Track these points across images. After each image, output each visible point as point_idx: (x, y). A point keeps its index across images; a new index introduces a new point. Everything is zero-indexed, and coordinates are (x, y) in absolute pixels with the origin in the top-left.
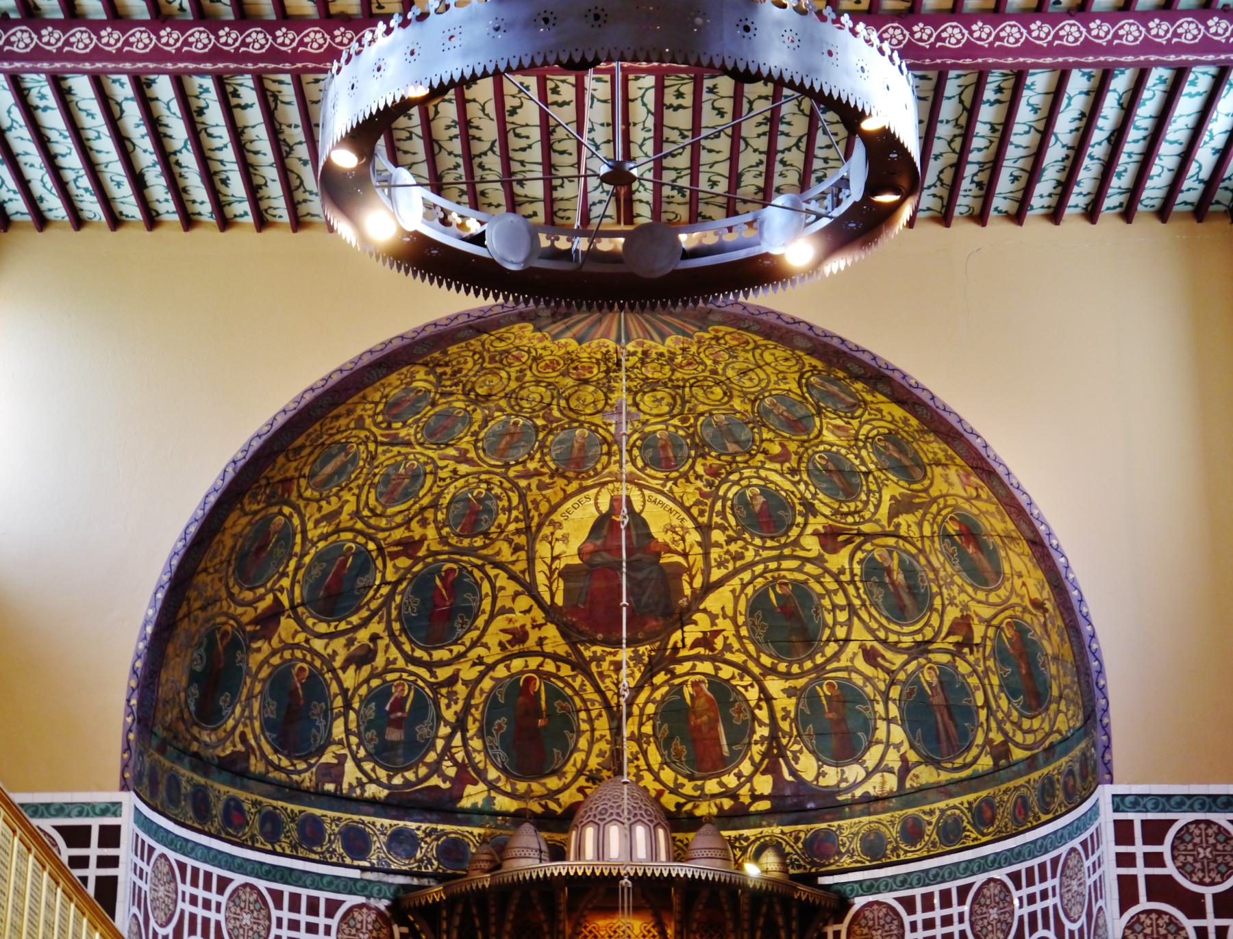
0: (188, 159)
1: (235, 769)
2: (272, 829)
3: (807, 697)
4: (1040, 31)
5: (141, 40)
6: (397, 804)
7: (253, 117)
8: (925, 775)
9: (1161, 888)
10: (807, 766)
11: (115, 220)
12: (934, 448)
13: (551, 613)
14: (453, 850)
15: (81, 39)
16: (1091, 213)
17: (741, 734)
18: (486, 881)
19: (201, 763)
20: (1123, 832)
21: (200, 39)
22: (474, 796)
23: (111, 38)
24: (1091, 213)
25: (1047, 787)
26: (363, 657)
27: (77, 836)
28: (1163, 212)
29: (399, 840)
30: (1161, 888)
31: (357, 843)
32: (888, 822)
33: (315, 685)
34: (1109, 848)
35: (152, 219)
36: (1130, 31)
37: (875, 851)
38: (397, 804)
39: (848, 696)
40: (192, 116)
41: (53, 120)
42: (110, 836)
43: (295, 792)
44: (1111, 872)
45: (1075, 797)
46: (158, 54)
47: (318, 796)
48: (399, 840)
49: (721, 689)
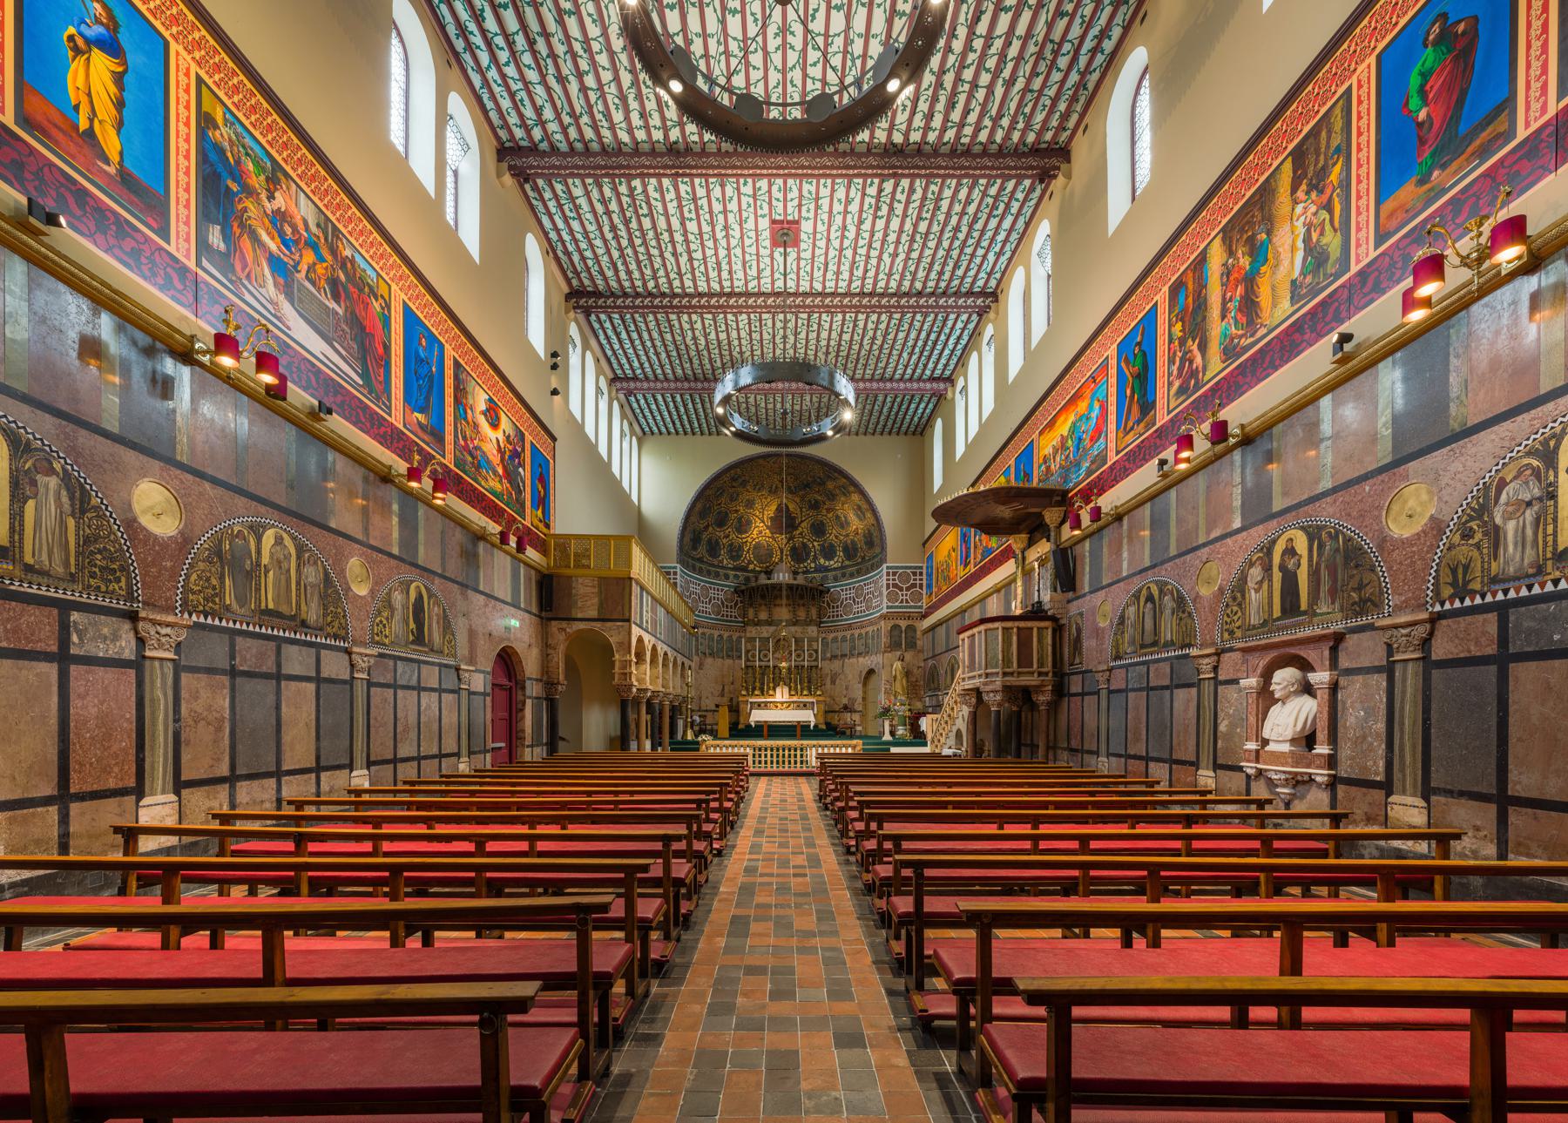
0: (685, 417)
1: (700, 560)
2: (709, 573)
3: (822, 546)
4: (881, 385)
5: (672, 385)
6: (735, 569)
7: (699, 406)
8: (847, 563)
9: (895, 586)
10: (822, 561)
11: (669, 433)
12: (852, 489)
13: (768, 527)
14: (747, 579)
15: (659, 385)
16: (890, 433)
17: (808, 555)
18: (754, 584)
19: (693, 559)
20: (888, 574)
21: (686, 385)
22: (751, 567)
23: (665, 384)
24: (890, 433)
25: (872, 565)
26: (727, 536)
27: (668, 573)
28: (906, 433)
29: (736, 576)
30: (895, 586)
31: (727, 577)
32: (838, 573)
33: (717, 543)
34: (885, 577)
35: (677, 433)
36: (902, 385)
37: (836, 579)
38: (735, 569)
39: (832, 546)
40: (685, 406)
41: (654, 407)
42: (675, 573)
43: (713, 566)
44: (885, 582)
45: (878, 567)
46: (676, 389)
47: (719, 567)
48: (736, 576)
49: (804, 545)
